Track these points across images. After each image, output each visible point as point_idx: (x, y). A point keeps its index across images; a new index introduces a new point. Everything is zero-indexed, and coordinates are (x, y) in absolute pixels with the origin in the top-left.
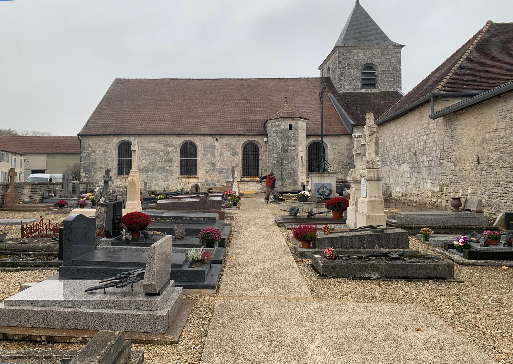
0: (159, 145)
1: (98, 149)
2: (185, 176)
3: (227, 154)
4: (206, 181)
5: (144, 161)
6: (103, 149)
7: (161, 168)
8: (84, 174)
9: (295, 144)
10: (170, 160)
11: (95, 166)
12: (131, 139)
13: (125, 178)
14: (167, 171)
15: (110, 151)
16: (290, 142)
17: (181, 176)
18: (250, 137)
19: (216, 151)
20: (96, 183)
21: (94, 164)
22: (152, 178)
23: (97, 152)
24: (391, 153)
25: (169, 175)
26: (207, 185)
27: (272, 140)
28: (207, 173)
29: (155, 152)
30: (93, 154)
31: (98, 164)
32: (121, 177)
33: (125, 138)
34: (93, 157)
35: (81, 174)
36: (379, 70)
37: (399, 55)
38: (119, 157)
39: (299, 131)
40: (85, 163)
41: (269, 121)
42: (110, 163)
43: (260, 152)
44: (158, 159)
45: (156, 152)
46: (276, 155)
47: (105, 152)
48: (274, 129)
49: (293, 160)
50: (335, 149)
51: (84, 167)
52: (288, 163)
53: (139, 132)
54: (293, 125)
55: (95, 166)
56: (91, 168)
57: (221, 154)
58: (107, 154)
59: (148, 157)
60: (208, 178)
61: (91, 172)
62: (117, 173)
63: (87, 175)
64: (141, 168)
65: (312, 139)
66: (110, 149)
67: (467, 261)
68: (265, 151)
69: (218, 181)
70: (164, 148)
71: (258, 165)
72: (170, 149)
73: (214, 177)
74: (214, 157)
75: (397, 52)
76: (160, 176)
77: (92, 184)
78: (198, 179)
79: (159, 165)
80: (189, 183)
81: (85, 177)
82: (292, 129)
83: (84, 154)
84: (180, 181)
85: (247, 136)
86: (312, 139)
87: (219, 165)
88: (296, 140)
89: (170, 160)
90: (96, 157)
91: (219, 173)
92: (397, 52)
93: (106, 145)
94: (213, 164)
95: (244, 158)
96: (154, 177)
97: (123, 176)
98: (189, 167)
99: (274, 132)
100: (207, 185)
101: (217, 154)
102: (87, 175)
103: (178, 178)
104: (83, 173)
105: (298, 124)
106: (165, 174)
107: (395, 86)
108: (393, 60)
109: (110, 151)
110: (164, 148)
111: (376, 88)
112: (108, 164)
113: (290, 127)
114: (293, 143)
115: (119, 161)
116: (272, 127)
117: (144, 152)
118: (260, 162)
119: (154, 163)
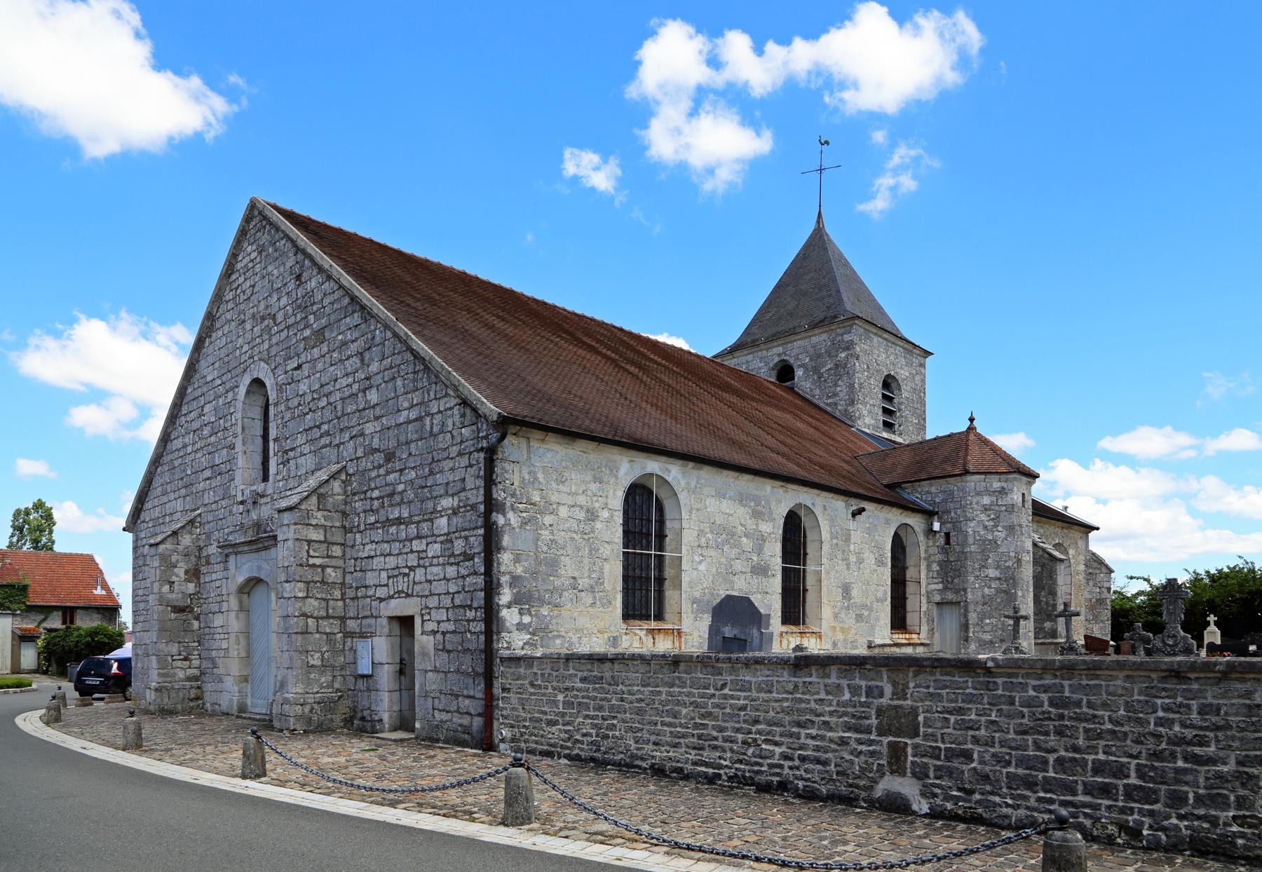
5: (702, 567)
6: (582, 500)
8: (515, 610)
12: (674, 472)
13: (651, 631)
15: (605, 514)
17: (784, 629)
19: (852, 547)
21: (553, 564)
23: (563, 512)
27: (980, 529)
30: (548, 520)
31: (568, 568)
34: (545, 533)
35: (504, 613)
41: (969, 478)
42: (607, 567)
46: (992, 573)
48: (986, 500)
51: (515, 580)
56: (542, 587)
58: (599, 525)
59: (713, 553)
61: (542, 602)
63: (527, 619)
64: (697, 595)
66: (605, 506)
67: (1036, 814)
70: (751, 524)
81: (520, 627)
83: (510, 515)
90: (560, 537)
94: (846, 590)
99: (986, 509)
101: (853, 559)
102: (527, 619)
109: (605, 514)
111: (894, 433)
112: (601, 569)
116: (979, 494)
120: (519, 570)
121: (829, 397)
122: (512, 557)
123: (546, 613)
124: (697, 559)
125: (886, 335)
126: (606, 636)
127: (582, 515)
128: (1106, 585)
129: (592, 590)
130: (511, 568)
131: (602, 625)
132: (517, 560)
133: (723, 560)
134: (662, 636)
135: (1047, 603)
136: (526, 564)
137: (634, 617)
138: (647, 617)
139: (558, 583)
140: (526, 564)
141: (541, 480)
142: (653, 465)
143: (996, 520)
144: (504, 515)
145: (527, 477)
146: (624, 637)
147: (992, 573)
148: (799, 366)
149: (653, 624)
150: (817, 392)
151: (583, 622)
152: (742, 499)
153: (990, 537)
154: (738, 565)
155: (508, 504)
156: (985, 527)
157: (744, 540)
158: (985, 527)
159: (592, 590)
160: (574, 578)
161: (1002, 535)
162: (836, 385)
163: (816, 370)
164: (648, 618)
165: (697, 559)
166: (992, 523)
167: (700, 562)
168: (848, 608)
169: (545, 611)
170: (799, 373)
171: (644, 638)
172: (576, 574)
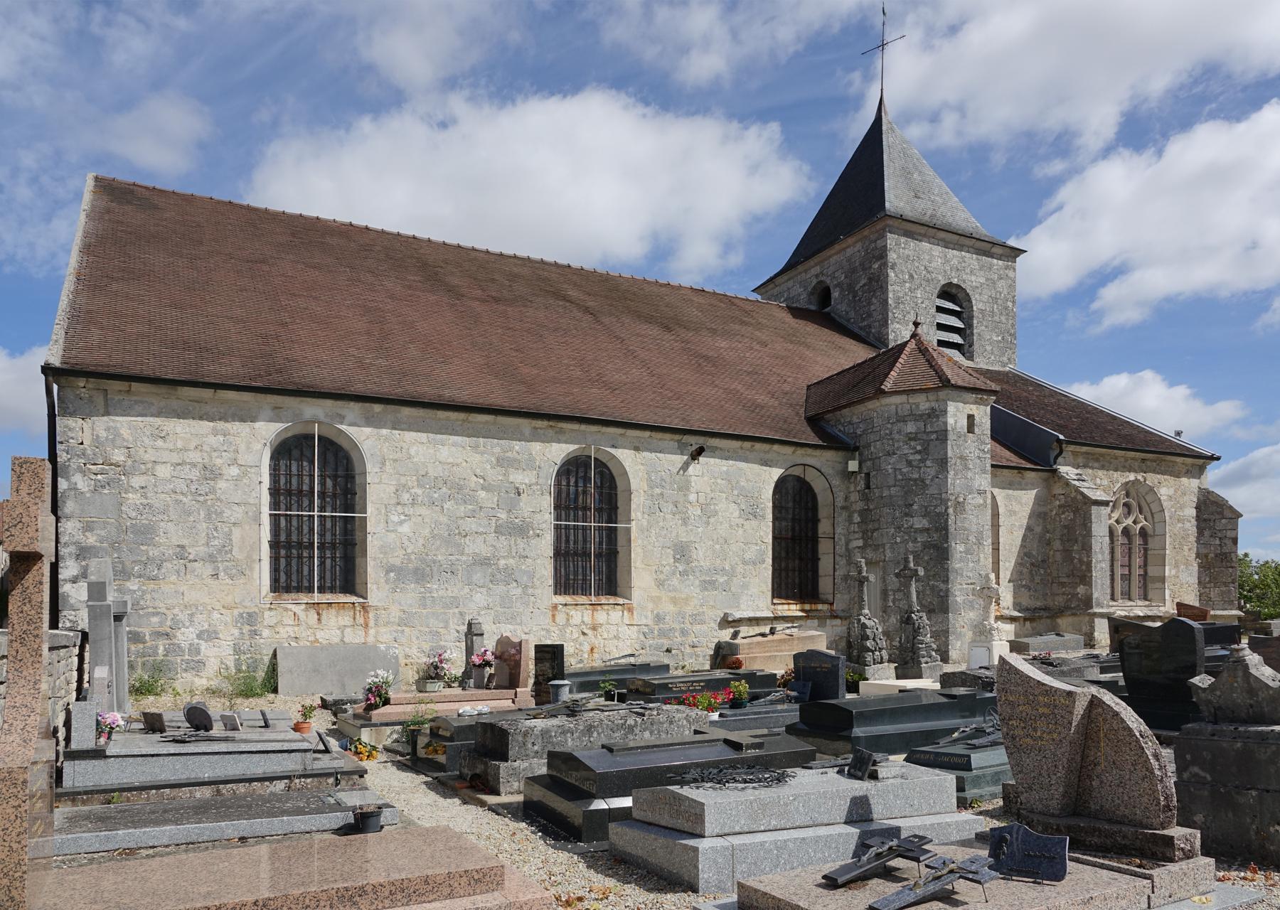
1: (165, 456)
2: (582, 599)
3: (729, 511)
4: (659, 618)
5: (405, 529)
7: (484, 562)
10: (522, 530)
11: (151, 542)
14: (509, 576)
16: (970, 474)
18: (800, 451)
19: (692, 497)
20: (158, 635)
21: (146, 533)
22: (446, 606)
25: (516, 591)
26: (662, 634)
28: (660, 584)
29: (458, 490)
31: (170, 534)
32: (296, 605)
33: (315, 415)
40: (88, 528)
42: (237, 533)
43: (823, 512)
44: (470, 525)
45: (460, 488)
47: (211, 474)
48: (911, 428)
50: (1015, 513)
54: (977, 418)
55: (151, 542)
57: (708, 512)
59: (424, 511)
60: (668, 608)
64: (397, 562)
66: (234, 462)
68: (843, 508)
69: (697, 619)
70: (494, 475)
72: (520, 478)
73: (687, 600)
74: (685, 522)
78: (630, 610)
79: (476, 547)
80: (594, 628)
82: (976, 430)
84: (561, 618)
85: (788, 450)
87: (702, 556)
89: (522, 530)
91: (708, 585)
93: (214, 441)
94: (682, 552)
97: (304, 598)
98: (591, 557)
99: (911, 438)
100: (662, 634)
101: (695, 511)
103: (555, 607)
104: (74, 580)
106: (501, 589)
107: (1005, 359)
108: (1001, 284)
110: (494, 475)
112: (230, 534)
116: (903, 420)
119: (453, 537)
120: (91, 540)
121: (863, 320)
122: (79, 525)
123: (135, 588)
124: (395, 518)
125: (942, 235)
126: (236, 612)
128: (1230, 534)
129: (211, 559)
130: (79, 537)
131: (230, 598)
133: (444, 519)
134: (333, 611)
135: (1081, 561)
136: (103, 533)
137: (288, 590)
138: (299, 589)
139: (153, 552)
140: (103, 533)
141: (126, 436)
142: (314, 410)
143: (925, 451)
144: (68, 479)
145: (103, 434)
146: (267, 614)
147: (920, 523)
148: (836, 286)
149: (316, 597)
150: (852, 314)
151: (192, 596)
153: (916, 476)
154: (470, 525)
155: (74, 466)
156: (909, 463)
157: (482, 494)
158: (909, 463)
159: (211, 559)
160: (182, 547)
161: (932, 472)
162: (870, 304)
163: (851, 288)
164: (310, 590)
165: (395, 518)
166: (918, 457)
167: (401, 523)
168: (684, 574)
170: (835, 294)
171: (302, 615)
172: (185, 542)
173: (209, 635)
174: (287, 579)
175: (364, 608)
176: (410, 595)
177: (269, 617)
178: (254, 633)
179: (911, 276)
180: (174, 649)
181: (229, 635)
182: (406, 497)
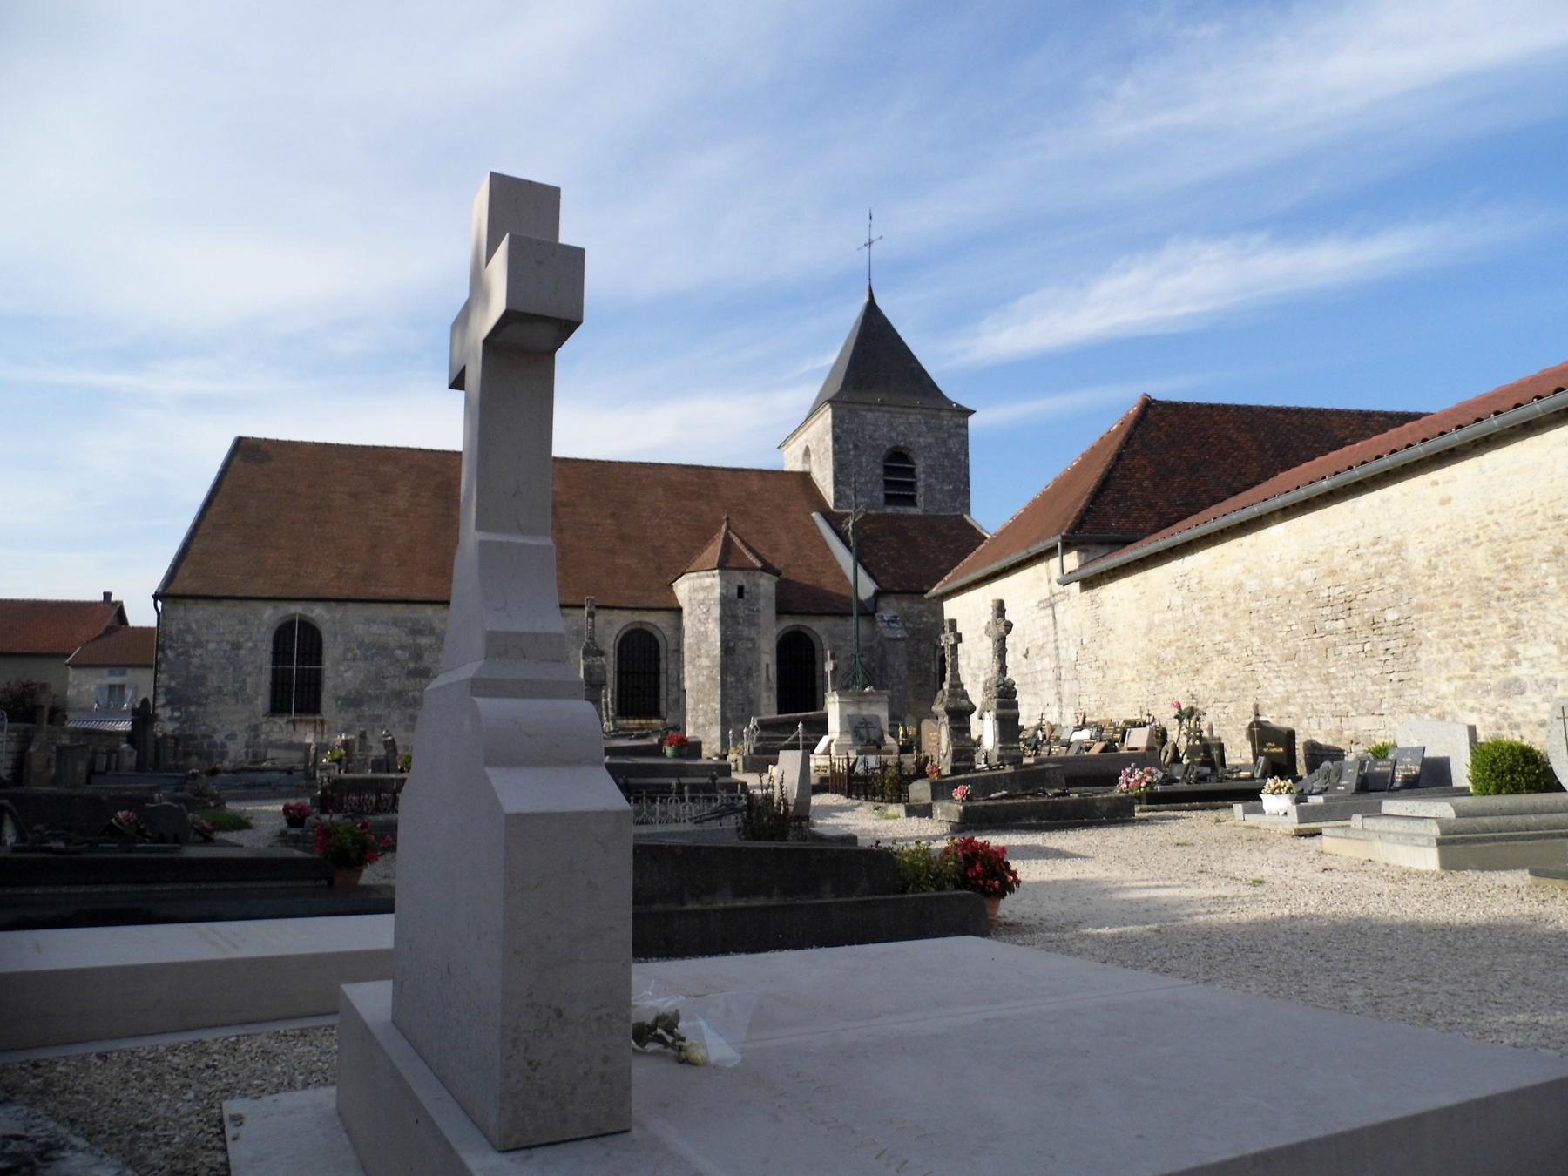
0: (393, 631)
5: (349, 674)
7: (399, 694)
9: (753, 633)
12: (317, 613)
13: (294, 722)
20: (204, 736)
21: (201, 680)
23: (212, 646)
24: (973, 655)
29: (381, 649)
30: (199, 652)
31: (213, 680)
32: (281, 721)
33: (296, 609)
34: (195, 661)
36: (920, 466)
37: (962, 431)
38: (275, 662)
39: (762, 603)
40: (172, 678)
42: (249, 680)
43: (662, 654)
44: (391, 671)
45: (385, 649)
47: (237, 646)
49: (749, 674)
51: (169, 691)
52: (739, 681)
53: (345, 594)
58: (243, 652)
59: (361, 664)
61: (190, 703)
62: (268, 706)
63: (177, 714)
65: (788, 623)
71: (657, 688)
72: (424, 641)
75: (959, 426)
76: (395, 717)
77: (193, 738)
79: (393, 684)
81: (172, 719)
86: (788, 623)
88: (753, 623)
92: (959, 426)
93: (239, 628)
95: (620, 668)
96: (378, 718)
102: (177, 714)
105: (757, 585)
106: (410, 710)
111: (915, 505)
113: (741, 590)
114: (747, 632)
115: (275, 672)
117: (349, 650)
118: (663, 678)
120: (173, 684)
127: (228, 647)
129: (235, 694)
132: (172, 678)
152: (395, 623)
157: (399, 652)
159: (235, 694)
164: (289, 712)
169: (192, 709)
173: (232, 737)
174: (278, 706)
175: (322, 722)
176: (350, 715)
177: (265, 727)
178: (256, 736)
179: (856, 447)
180: (214, 745)
181: (242, 737)
182: (350, 656)
